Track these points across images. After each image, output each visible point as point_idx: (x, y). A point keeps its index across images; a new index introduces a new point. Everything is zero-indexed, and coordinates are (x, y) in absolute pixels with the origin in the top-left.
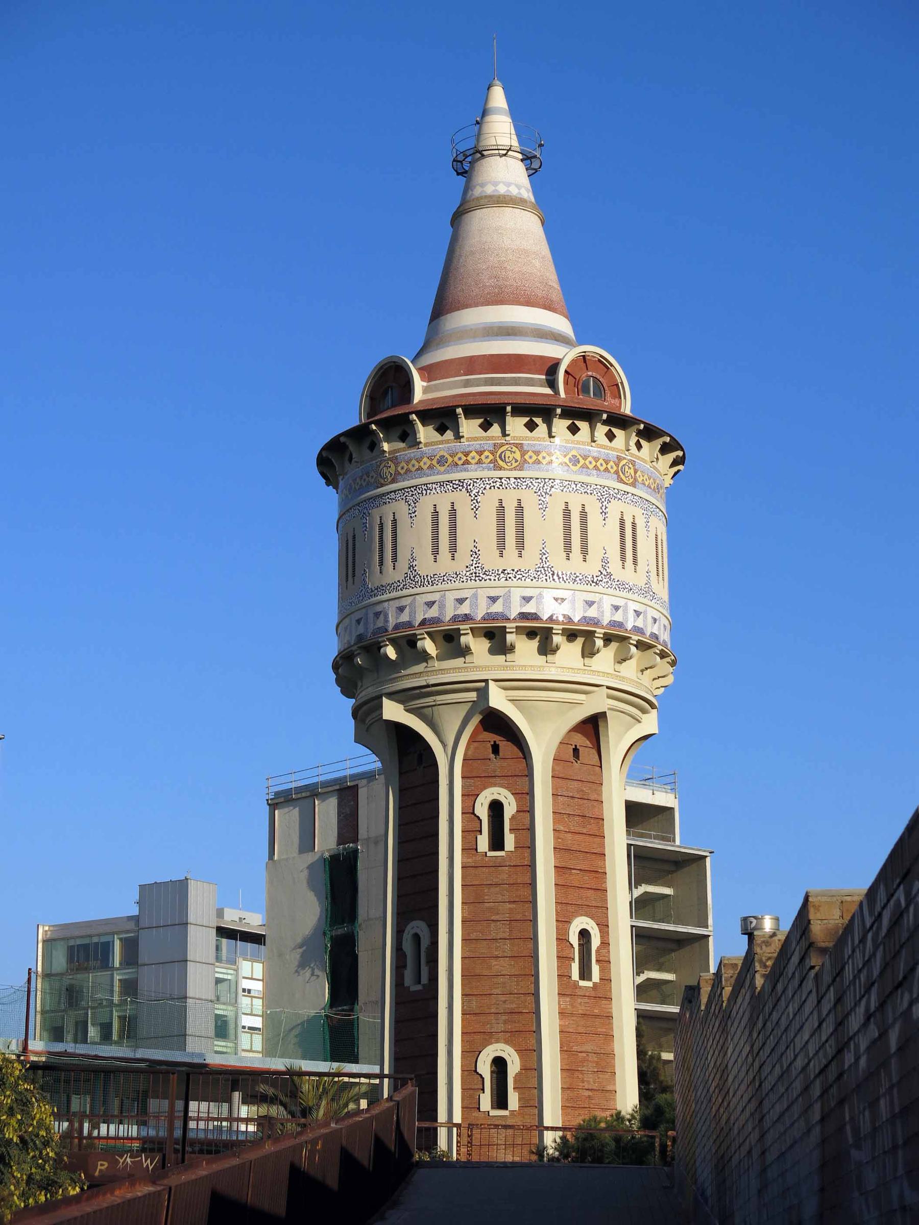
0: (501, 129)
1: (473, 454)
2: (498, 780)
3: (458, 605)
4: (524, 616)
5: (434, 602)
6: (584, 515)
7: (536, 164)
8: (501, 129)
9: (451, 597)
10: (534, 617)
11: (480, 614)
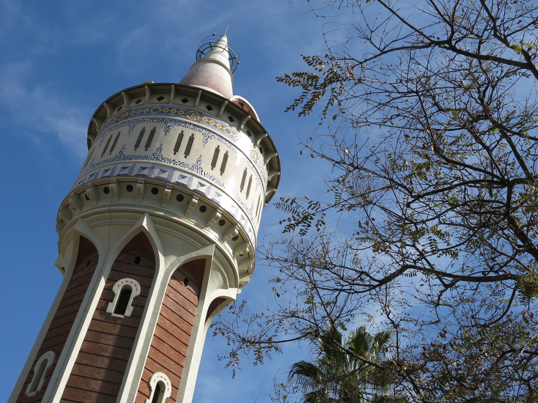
4: (178, 183)
5: (127, 168)
9: (137, 167)
10: (185, 186)
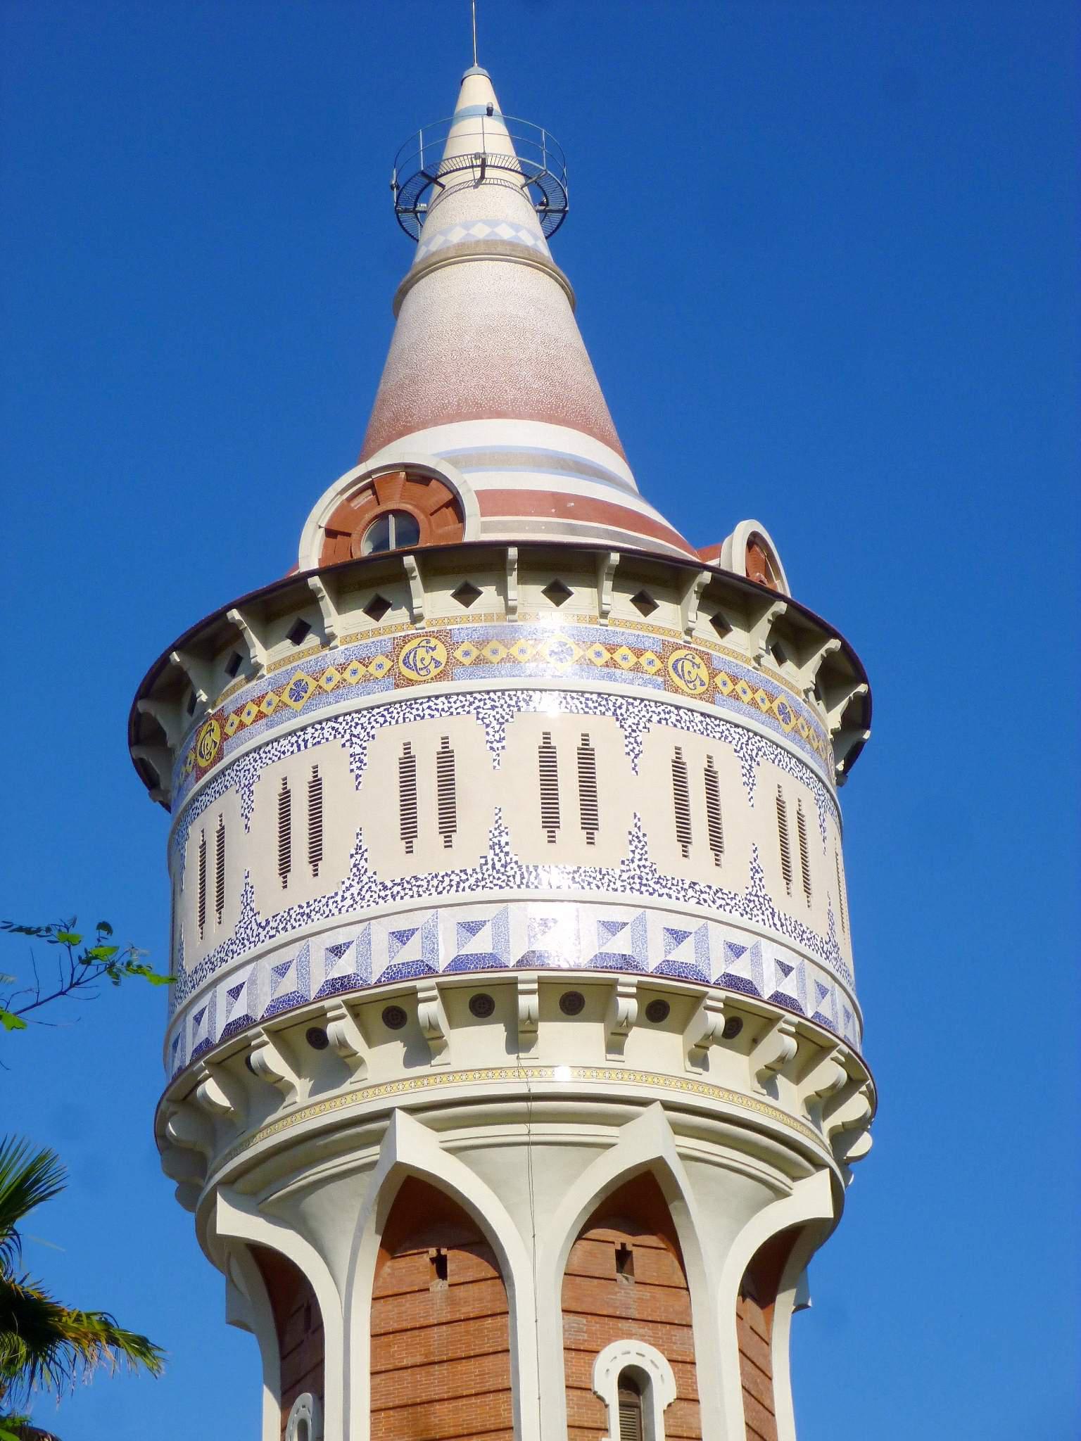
1: (624, 651)
2: (633, 1326)
3: (608, 935)
4: (732, 982)
10: (748, 987)
11: (653, 961)
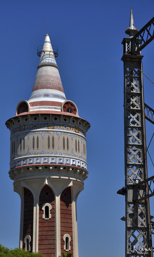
0: (48, 47)
6: (68, 139)
7: (57, 55)
8: (48, 47)
